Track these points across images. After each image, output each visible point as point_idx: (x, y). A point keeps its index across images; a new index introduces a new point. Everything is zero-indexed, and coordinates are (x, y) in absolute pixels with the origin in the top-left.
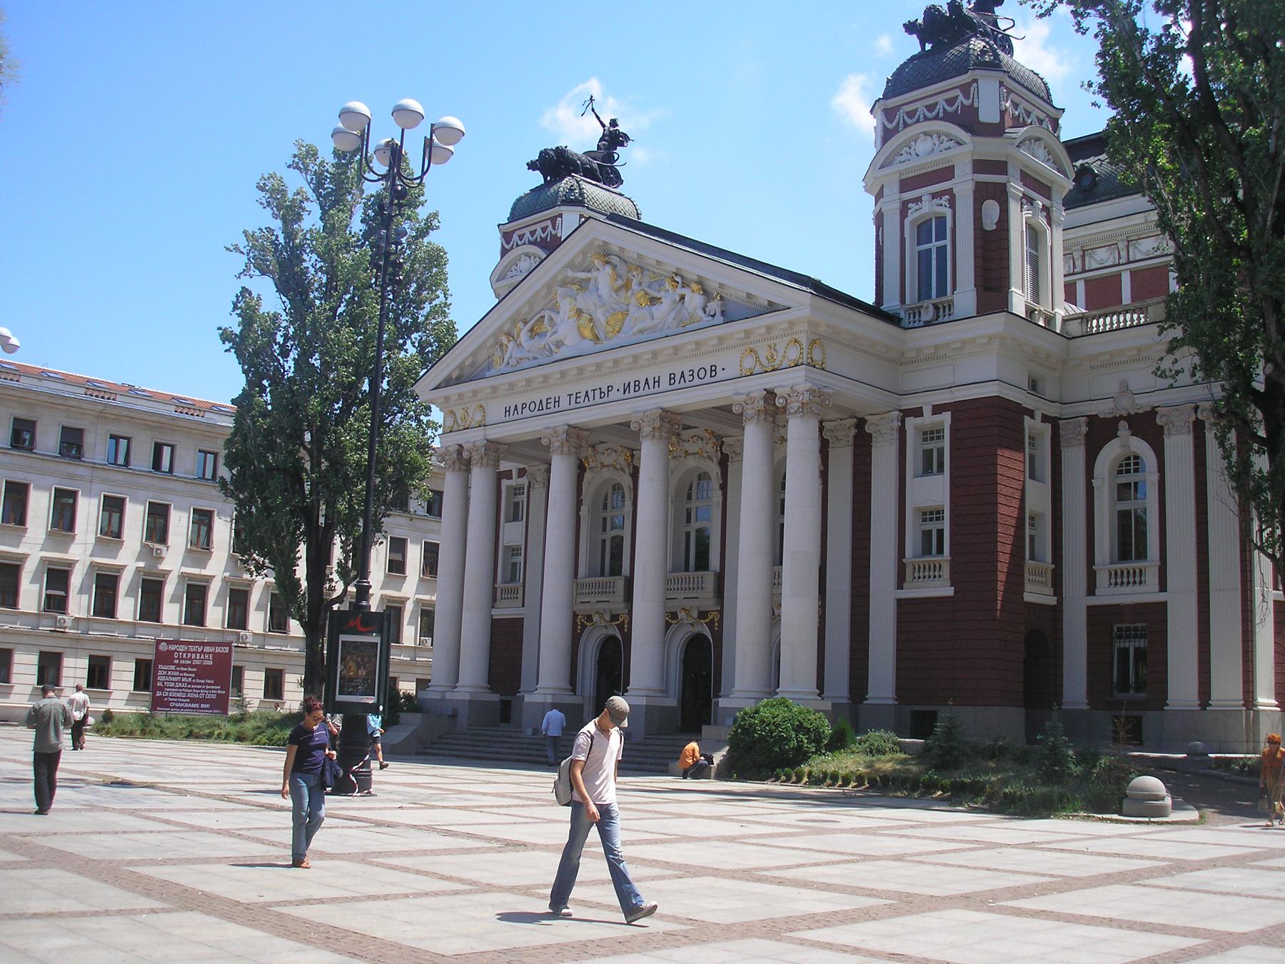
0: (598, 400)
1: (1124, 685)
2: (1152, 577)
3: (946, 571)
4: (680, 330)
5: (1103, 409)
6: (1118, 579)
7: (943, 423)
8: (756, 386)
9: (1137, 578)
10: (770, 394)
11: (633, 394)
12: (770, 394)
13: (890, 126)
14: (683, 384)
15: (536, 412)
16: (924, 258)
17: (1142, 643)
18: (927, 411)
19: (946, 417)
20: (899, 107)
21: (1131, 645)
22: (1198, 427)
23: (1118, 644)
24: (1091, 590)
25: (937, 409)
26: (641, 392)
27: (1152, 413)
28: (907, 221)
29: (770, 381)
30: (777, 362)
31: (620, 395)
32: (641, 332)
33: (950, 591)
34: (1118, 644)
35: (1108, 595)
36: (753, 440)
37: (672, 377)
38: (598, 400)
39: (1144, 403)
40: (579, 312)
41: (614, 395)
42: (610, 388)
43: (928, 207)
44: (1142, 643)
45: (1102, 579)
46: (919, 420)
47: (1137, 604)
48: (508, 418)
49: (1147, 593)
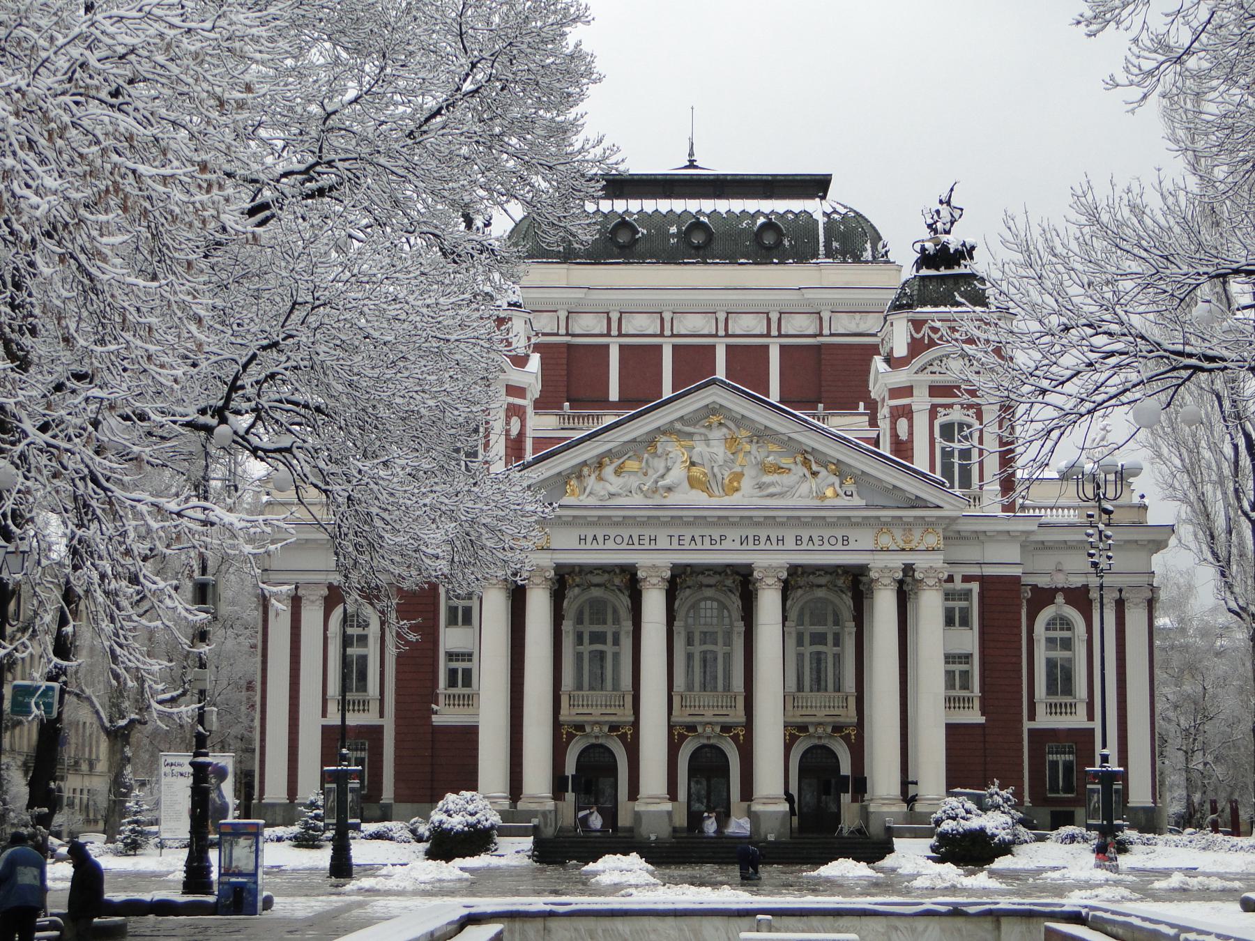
0: (707, 545)
1: (1054, 789)
2: (1082, 710)
3: (977, 703)
4: (817, 503)
5: (1043, 582)
6: (1053, 709)
7: (971, 590)
8: (898, 561)
9: (1070, 708)
10: (908, 569)
11: (751, 546)
12: (908, 569)
13: (916, 336)
14: (811, 547)
15: (624, 546)
16: (947, 455)
17: (1071, 757)
18: (958, 578)
19: (975, 587)
20: (926, 321)
21: (1061, 758)
22: (1120, 605)
23: (1051, 757)
24: (1032, 717)
25: (966, 579)
26: (762, 547)
27: (1085, 589)
28: (937, 424)
29: (908, 558)
30: (913, 545)
31: (737, 545)
32: (772, 495)
33: (982, 720)
34: (1051, 757)
35: (1044, 720)
36: (884, 604)
37: (798, 539)
38: (707, 545)
39: (1077, 581)
40: (693, 464)
41: (727, 544)
42: (723, 538)
43: (956, 415)
44: (1071, 757)
45: (1041, 709)
46: (950, 585)
47: (1069, 730)
48: (582, 546)
49: (1078, 720)
